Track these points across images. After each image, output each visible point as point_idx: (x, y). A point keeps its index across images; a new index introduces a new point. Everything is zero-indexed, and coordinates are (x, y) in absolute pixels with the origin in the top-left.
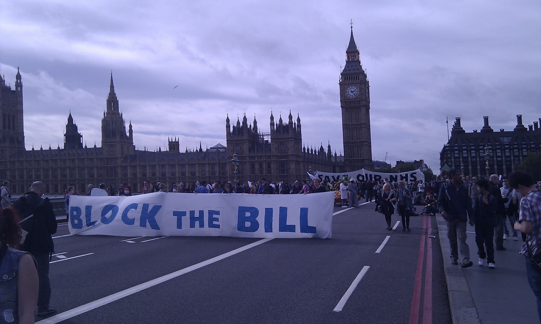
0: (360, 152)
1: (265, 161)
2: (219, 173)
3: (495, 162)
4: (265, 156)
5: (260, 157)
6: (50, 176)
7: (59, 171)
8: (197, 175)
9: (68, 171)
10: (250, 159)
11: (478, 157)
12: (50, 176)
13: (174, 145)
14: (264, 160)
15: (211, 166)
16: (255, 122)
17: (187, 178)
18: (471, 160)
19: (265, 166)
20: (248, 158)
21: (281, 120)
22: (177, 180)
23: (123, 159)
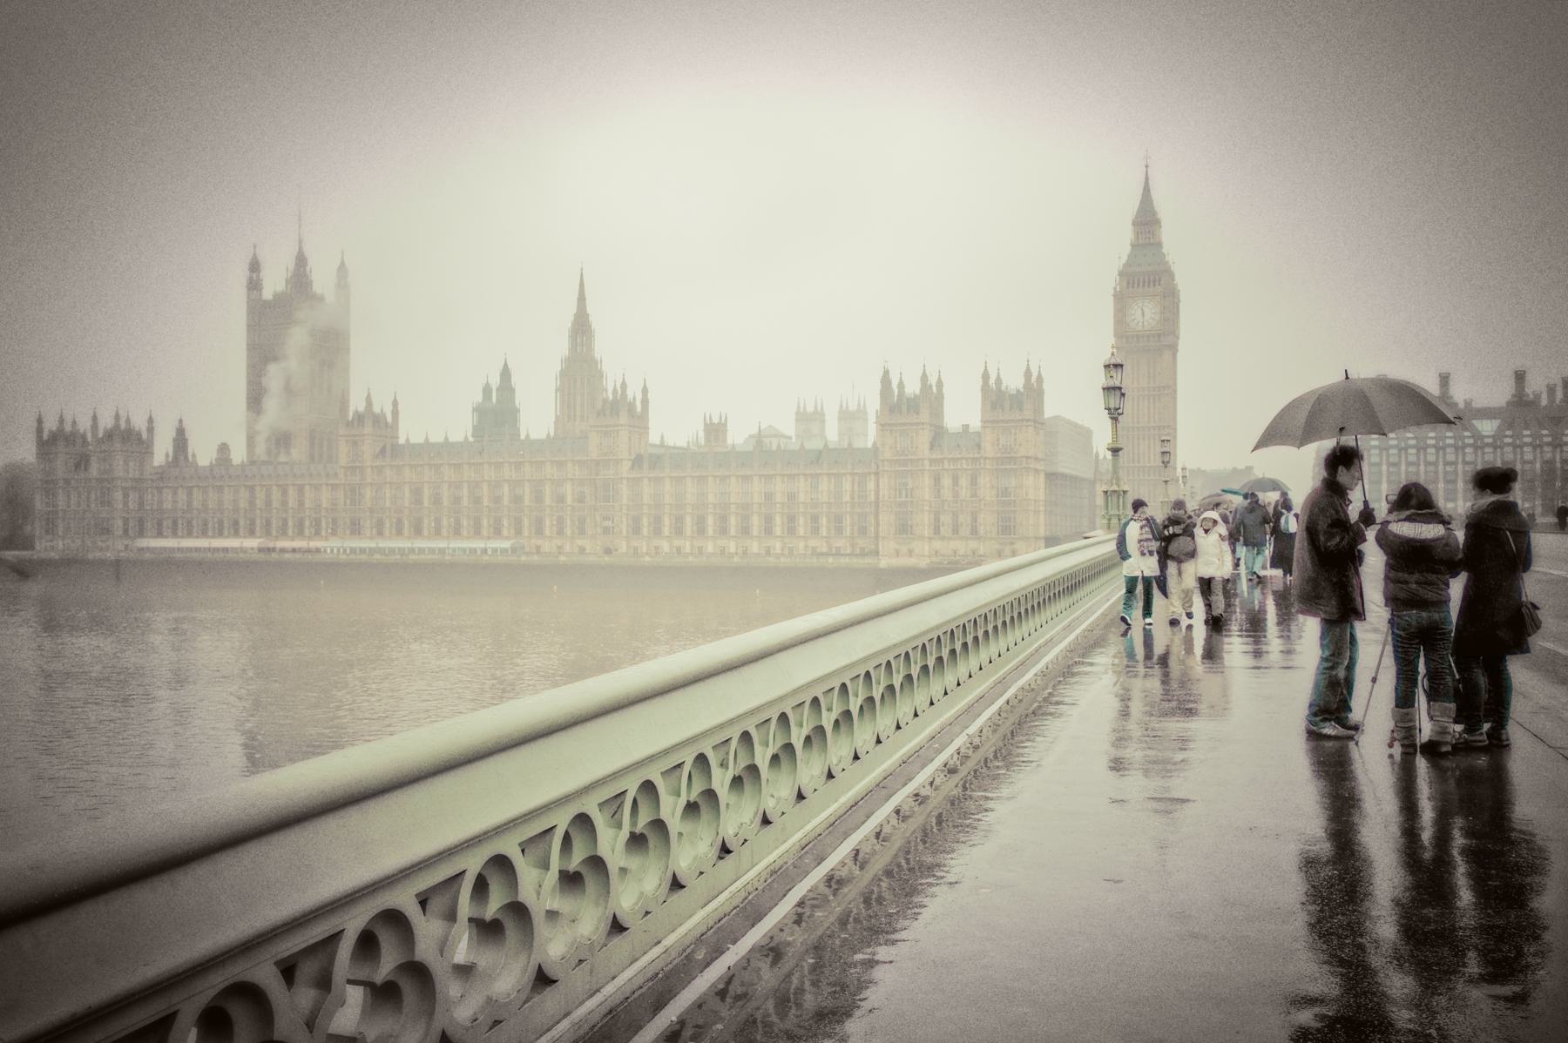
0: (1155, 450)
1: (966, 470)
2: (852, 498)
3: (1441, 476)
4: (966, 459)
5: (954, 460)
6: (465, 499)
7: (485, 487)
8: (802, 497)
9: (506, 489)
10: (930, 466)
11: (1422, 463)
12: (465, 499)
13: (715, 430)
14: (965, 466)
15: (833, 480)
16: (940, 384)
17: (778, 505)
18: (1406, 470)
19: (964, 481)
20: (927, 463)
21: (999, 380)
22: (666, 511)
23: (630, 463)
